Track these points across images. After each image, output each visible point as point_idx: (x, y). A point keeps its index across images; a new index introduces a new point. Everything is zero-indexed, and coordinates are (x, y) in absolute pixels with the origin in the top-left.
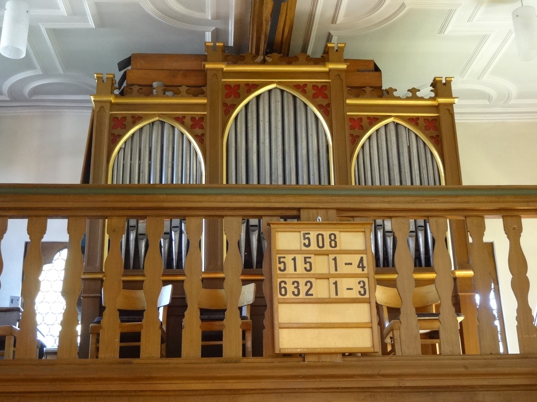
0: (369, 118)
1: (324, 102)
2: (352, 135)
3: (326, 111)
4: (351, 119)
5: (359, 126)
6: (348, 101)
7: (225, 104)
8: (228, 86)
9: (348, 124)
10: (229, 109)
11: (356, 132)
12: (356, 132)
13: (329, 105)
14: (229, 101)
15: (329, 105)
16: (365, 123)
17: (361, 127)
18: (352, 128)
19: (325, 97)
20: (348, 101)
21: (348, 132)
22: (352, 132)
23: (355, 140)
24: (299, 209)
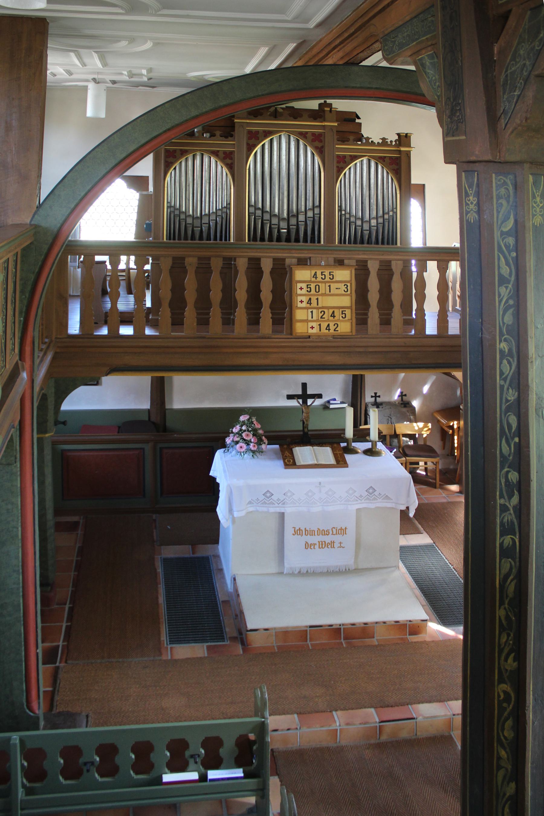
0: (351, 156)
1: (320, 145)
2: (338, 167)
3: (320, 151)
4: (338, 156)
5: (343, 162)
6: (337, 146)
7: (248, 144)
8: (250, 132)
9: (335, 160)
10: (250, 148)
11: (341, 165)
12: (341, 165)
13: (322, 147)
14: (251, 142)
15: (322, 147)
16: (347, 159)
17: (345, 162)
18: (338, 162)
19: (321, 141)
20: (337, 146)
21: (335, 164)
22: (338, 165)
23: (340, 170)
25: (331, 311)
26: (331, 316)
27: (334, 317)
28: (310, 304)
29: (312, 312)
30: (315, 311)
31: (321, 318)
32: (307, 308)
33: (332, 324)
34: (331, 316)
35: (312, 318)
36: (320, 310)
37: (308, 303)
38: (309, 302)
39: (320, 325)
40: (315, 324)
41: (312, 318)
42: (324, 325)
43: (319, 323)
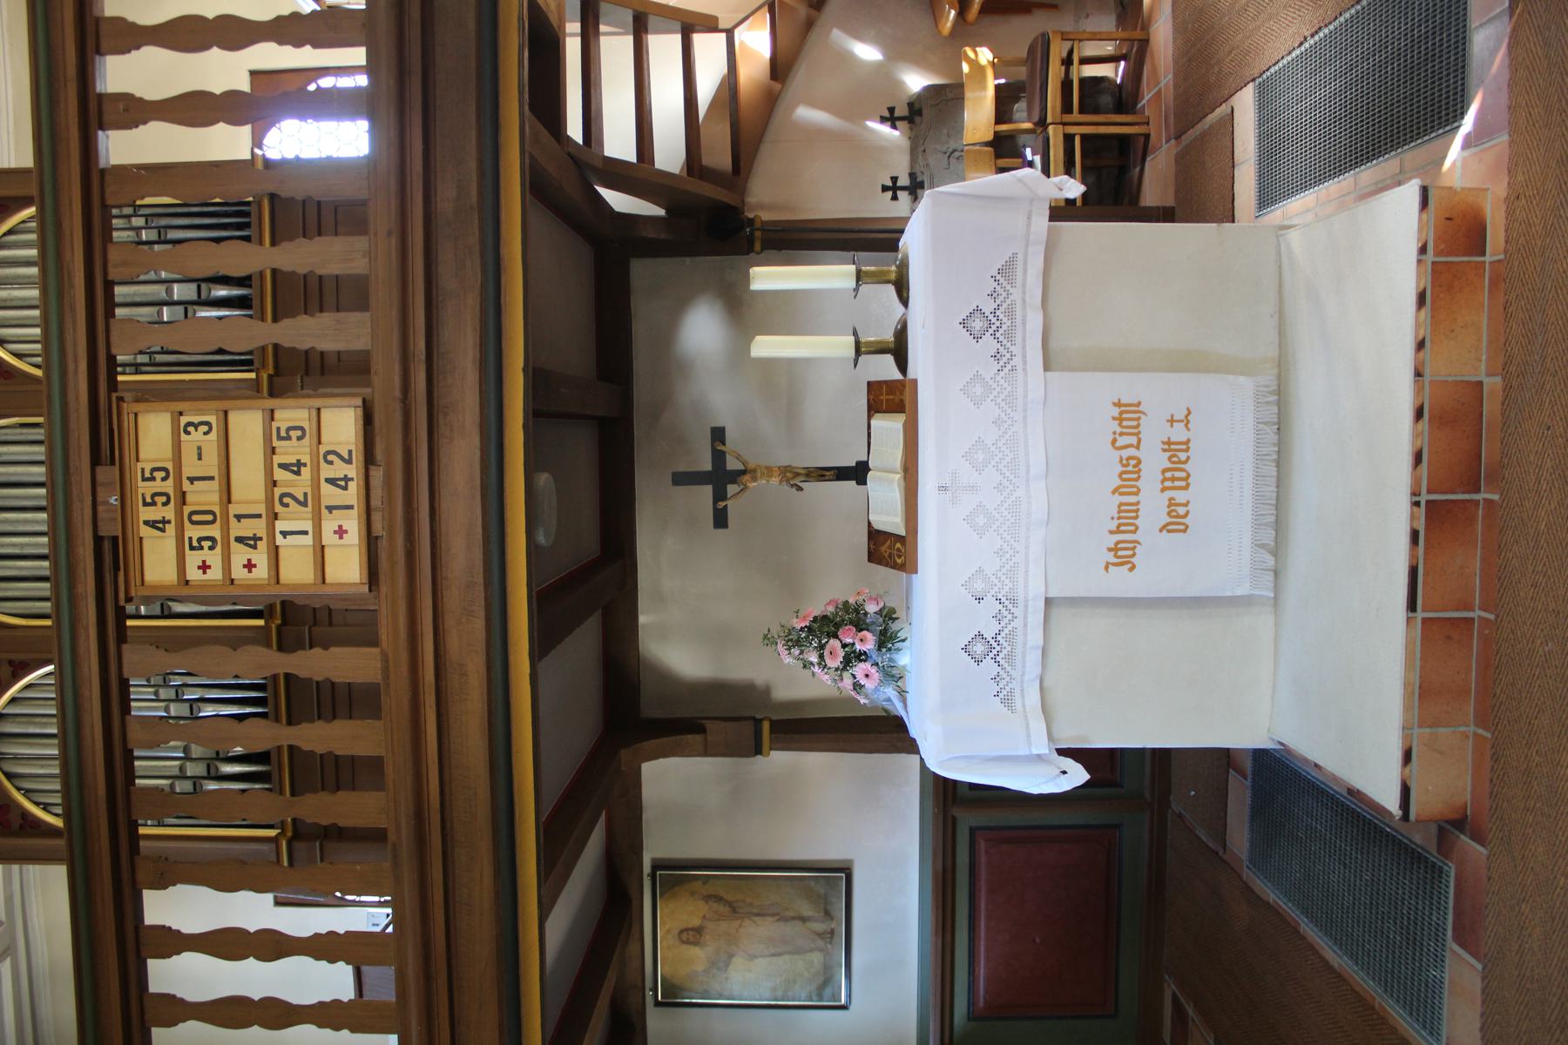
24: (98, 540)
25: (280, 475)
26: (298, 473)
27: (299, 464)
28: (256, 539)
29: (284, 534)
30: (280, 525)
31: (304, 504)
32: (275, 551)
33: (327, 472)
34: (298, 473)
35: (306, 533)
36: (278, 508)
37: (255, 547)
38: (250, 542)
39: (330, 509)
40: (329, 526)
41: (306, 533)
42: (330, 494)
43: (325, 512)
